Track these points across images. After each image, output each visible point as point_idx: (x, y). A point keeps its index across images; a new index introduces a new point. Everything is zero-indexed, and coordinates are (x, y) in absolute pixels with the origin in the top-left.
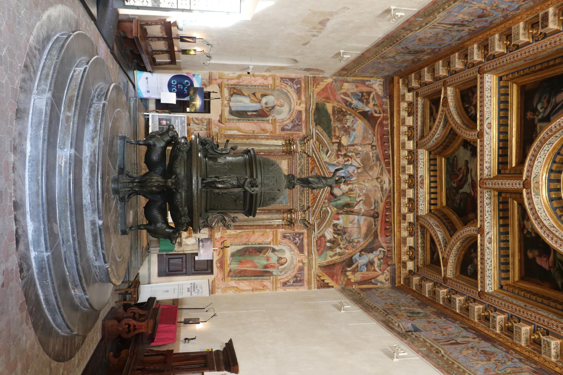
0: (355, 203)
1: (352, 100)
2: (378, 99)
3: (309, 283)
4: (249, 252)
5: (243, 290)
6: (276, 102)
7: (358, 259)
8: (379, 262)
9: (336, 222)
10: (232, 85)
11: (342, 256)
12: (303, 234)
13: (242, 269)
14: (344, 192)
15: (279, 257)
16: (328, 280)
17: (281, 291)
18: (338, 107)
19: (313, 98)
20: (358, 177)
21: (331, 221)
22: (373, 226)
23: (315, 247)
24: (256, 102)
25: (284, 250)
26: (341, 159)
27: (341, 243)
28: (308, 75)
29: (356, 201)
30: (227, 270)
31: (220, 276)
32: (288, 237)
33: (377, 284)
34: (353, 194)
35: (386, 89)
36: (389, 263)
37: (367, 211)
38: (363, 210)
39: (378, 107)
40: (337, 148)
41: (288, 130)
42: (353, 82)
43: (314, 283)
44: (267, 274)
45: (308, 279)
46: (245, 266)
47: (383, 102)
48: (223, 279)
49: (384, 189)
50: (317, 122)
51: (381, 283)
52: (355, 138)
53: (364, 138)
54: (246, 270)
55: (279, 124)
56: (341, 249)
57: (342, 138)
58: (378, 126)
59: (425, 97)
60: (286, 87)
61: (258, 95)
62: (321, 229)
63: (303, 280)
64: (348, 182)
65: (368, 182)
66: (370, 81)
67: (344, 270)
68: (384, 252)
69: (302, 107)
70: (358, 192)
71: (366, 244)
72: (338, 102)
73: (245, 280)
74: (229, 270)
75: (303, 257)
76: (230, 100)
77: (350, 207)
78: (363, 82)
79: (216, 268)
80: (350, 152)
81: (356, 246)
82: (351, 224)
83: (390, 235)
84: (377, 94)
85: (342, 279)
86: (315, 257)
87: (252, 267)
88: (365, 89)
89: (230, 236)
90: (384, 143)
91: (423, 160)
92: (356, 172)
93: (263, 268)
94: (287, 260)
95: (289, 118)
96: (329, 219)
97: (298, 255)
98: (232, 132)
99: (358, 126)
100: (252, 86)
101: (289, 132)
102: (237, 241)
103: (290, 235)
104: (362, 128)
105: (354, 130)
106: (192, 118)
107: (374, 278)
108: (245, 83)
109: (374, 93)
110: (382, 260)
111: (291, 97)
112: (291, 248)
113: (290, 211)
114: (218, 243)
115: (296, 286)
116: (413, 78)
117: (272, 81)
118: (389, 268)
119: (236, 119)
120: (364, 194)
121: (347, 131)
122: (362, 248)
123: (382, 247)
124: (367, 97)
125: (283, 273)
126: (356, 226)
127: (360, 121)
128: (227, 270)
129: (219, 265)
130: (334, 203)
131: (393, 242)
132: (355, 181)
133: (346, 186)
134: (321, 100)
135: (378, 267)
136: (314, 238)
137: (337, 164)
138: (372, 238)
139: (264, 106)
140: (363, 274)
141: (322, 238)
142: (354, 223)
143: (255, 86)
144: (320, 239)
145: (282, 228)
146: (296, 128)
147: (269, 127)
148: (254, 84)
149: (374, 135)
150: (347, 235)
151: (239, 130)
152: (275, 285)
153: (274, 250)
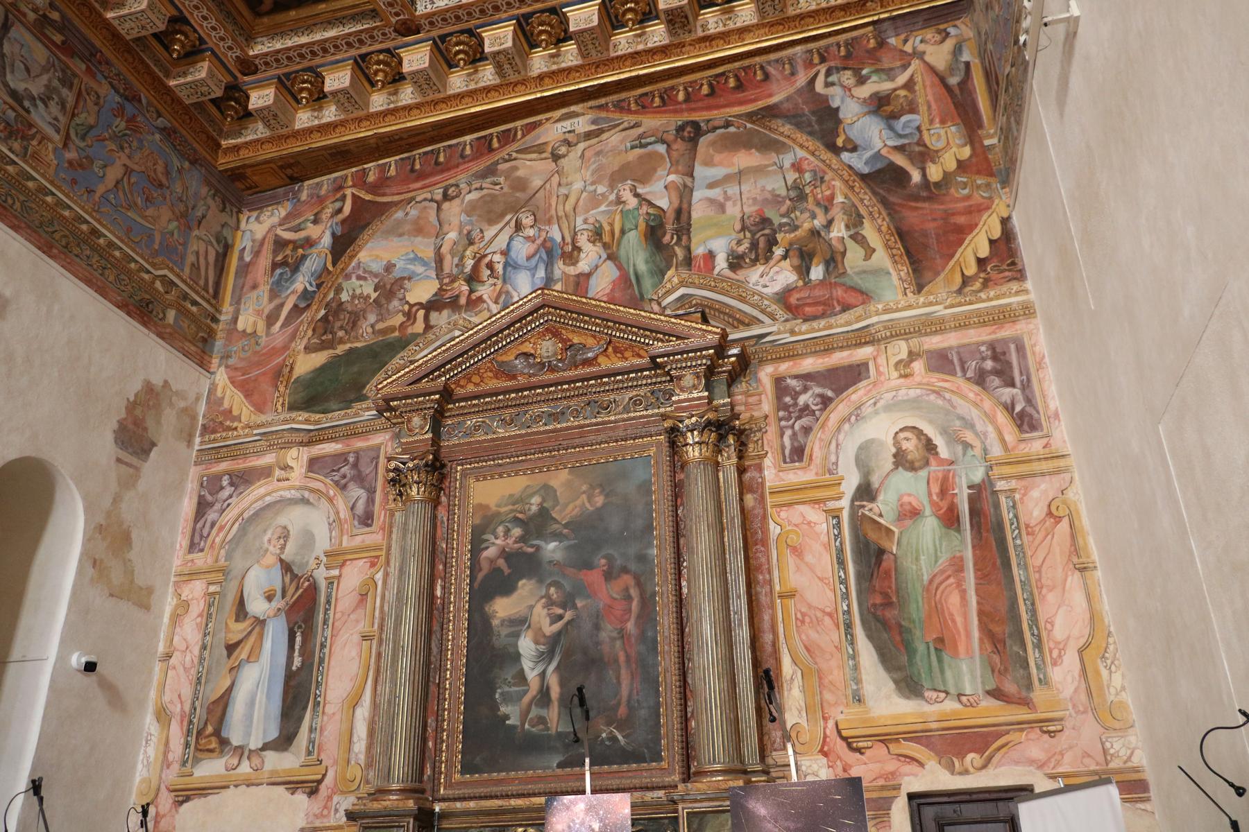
0: (645, 209)
1: (293, 292)
2: (299, 215)
3: (1004, 316)
4: (888, 604)
5: (1094, 617)
6: (270, 559)
7: (868, 154)
8: (874, 78)
9: (721, 263)
10: (187, 745)
11: (863, 211)
12: (778, 381)
13: (976, 634)
14: (604, 256)
15: (897, 464)
16: (979, 244)
17: (1062, 435)
18: (310, 333)
19: (270, 424)
20: (549, 222)
21: (724, 279)
22: (732, 129)
23: (832, 320)
24: (261, 636)
25: (861, 448)
26: (485, 291)
27: (807, 226)
28: (195, 453)
30: (992, 712)
31: (1034, 746)
32: (801, 438)
33: (967, 64)
34: (611, 225)
35: (274, 197)
36: (872, 43)
38: (672, 177)
39: (323, 209)
40: (445, 312)
41: (371, 501)
42: (237, 301)
43: (997, 297)
44: (988, 508)
45: (984, 324)
46: (959, 620)
47: (311, 196)
48: (1048, 727)
49: (594, 127)
50: (352, 396)
51: (957, 50)
52: (417, 259)
53: (419, 230)
54: (981, 613)
55: (345, 538)
56: (830, 223)
57: (412, 302)
58: (384, 195)
59: (250, 39)
60: (221, 528)
61: (238, 630)
62: (755, 313)
63: (992, 346)
66: (245, 248)
67: (924, 194)
68: (829, 73)
69: (297, 458)
70: (603, 208)
71: (801, 137)
72: (293, 337)
73: (1033, 613)
75: (882, 360)
76: (240, 750)
77: (662, 225)
78: (244, 269)
79: (990, 770)
80: (460, 265)
81: (814, 172)
82: (729, 204)
83: (762, 68)
85: (966, 192)
86: (877, 313)
87: (959, 585)
88: (265, 261)
89: (815, 708)
90: (437, 163)
92: (531, 232)
93: (958, 530)
94: (901, 430)
95: (330, 500)
97: (875, 384)
98: (361, 730)
100: (201, 659)
101: (378, 497)
102: (836, 672)
103: (788, 432)
104: (384, 242)
105: (389, 267)
107: (943, 80)
108: (187, 692)
109: (279, 232)
110: (864, 72)
112: (846, 419)
113: (674, 437)
115: (1025, 371)
116: (182, 80)
117: (198, 583)
118: (892, 41)
119: (312, 719)
120: (612, 187)
121: (390, 287)
122: (822, 147)
123: (812, 81)
124: (288, 252)
125: (969, 437)
126: (733, 190)
127: (363, 256)
128: (992, 712)
130: (647, 283)
132: (565, 225)
133: (582, 255)
134: (282, 394)
135: (892, 79)
136: (792, 333)
137: (503, 296)
138: (777, 123)
139: (278, 603)
140: (931, 122)
141: (793, 300)
142: (721, 199)
143: (204, 647)
144: (797, 307)
145: (760, 468)
146: (366, 469)
147: (353, 576)
148: (196, 651)
149: (413, 199)
150: (770, 213)
152: (1036, 467)
153: (866, 492)
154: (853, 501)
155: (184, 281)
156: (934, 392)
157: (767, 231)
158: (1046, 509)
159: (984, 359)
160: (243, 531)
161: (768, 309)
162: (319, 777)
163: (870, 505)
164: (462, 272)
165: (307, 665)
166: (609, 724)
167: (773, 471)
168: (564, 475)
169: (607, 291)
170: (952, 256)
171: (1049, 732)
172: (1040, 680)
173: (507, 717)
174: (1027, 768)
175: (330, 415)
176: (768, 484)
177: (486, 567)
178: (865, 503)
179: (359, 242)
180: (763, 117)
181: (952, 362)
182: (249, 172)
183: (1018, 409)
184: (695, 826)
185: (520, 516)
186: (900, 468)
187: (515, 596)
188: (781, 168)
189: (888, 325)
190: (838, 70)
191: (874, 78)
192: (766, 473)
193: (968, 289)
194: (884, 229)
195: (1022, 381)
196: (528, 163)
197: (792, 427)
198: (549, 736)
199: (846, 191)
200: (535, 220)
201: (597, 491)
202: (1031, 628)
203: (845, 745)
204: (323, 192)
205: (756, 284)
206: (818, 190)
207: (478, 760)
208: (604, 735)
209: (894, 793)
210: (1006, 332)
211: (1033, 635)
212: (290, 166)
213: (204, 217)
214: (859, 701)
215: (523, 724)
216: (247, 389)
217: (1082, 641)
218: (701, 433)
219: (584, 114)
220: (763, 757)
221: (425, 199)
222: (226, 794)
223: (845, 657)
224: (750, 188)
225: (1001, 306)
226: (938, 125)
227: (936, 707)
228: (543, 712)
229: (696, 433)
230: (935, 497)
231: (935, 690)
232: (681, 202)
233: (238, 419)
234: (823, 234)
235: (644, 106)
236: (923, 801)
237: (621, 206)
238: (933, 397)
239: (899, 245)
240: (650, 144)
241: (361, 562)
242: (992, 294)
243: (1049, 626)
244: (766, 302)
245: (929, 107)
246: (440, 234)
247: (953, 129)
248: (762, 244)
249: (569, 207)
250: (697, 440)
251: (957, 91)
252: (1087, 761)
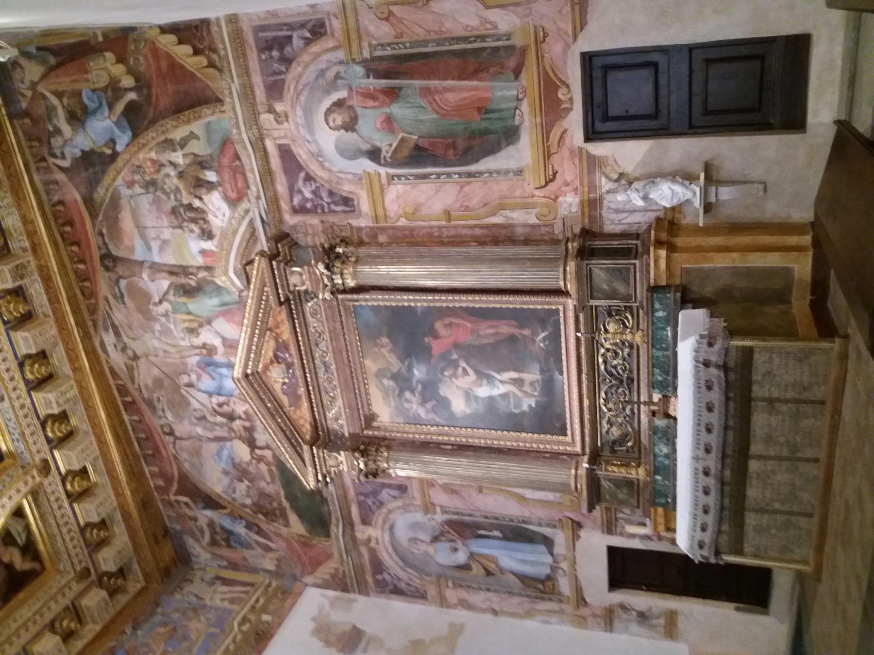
0: (171, 297)
4: (454, 146)
6: (430, 549)
7: (116, 130)
9: (208, 245)
10: (550, 600)
11: (162, 138)
12: (295, 211)
13: (475, 83)
14: (208, 327)
15: (353, 130)
18: (275, 524)
20: (185, 364)
21: (220, 245)
22: (104, 231)
23: (247, 168)
24: (480, 555)
27: (175, 181)
29: (171, 303)
30: (530, 77)
31: (554, 49)
32: (337, 198)
34: (184, 321)
36: (27, 121)
37: (133, 275)
38: (145, 276)
40: (256, 435)
43: (223, 42)
44: (383, 66)
45: (244, 55)
46: (465, 95)
48: (541, 38)
49: (111, 330)
52: (219, 454)
53: (197, 453)
54: (460, 78)
55: (415, 502)
56: (171, 163)
58: (173, 476)
60: (411, 580)
61: (477, 569)
63: (261, 50)
64: (204, 351)
65: (155, 349)
67: (145, 91)
68: (54, 156)
70: (172, 327)
71: (107, 180)
72: (279, 535)
74: (523, 76)
75: (276, 134)
76: (554, 568)
79: (570, 81)
80: (221, 425)
81: (134, 172)
83: (54, 205)
84: (198, 541)
86: (240, 134)
88: (226, 552)
90: (147, 439)
92: (194, 377)
93: (400, 89)
94: (328, 124)
95: (390, 512)
96: (229, 253)
97: (294, 141)
100: (496, 591)
103: (333, 207)
105: (226, 473)
108: (516, 600)
110: (51, 129)
111: (395, 557)
112: (322, 165)
114: (569, 179)
115: (280, 27)
120: (155, 319)
121: (241, 472)
124: (218, 538)
125: (331, 74)
126: (152, 233)
128: (530, 77)
129: (561, 94)
130: (227, 298)
131: (39, 184)
133: (209, 342)
134: (320, 543)
139: (459, 544)
140: (87, 80)
142: (159, 242)
143: (488, 590)
144: (238, 192)
145: (359, 229)
148: (491, 594)
149: (174, 456)
151: (522, 499)
153: (374, 154)
154: (380, 164)
155: (242, 608)
156: (298, 97)
157: (182, 210)
158: (384, 22)
159: (271, 57)
160: (413, 566)
161: (242, 213)
162: (570, 521)
163: (384, 153)
164: (226, 425)
165: (499, 528)
166: (534, 341)
167: (361, 220)
168: (368, 363)
169: (235, 326)
170: (193, 74)
171: (544, 37)
172: (507, 39)
173: (530, 406)
174: (569, 55)
175: (332, 511)
176: (371, 224)
177: (431, 416)
178: (382, 156)
179: (209, 492)
180: (93, 207)
181: (275, 82)
182: (162, 565)
183: (308, 35)
184: (600, 296)
185: (397, 392)
186: (356, 127)
187: (450, 397)
188: (131, 197)
189: (249, 128)
190: (50, 148)
191: (55, 121)
192: (363, 225)
193: (218, 64)
194: (174, 123)
195: (288, 30)
196: (141, 377)
197: (329, 204)
198: (543, 380)
199: (146, 149)
200: (185, 373)
201: (378, 341)
202: (470, 42)
203: (550, 184)
204: (174, 515)
205: (223, 221)
206: (147, 170)
207: (558, 425)
208: (542, 345)
209: (584, 152)
210: (250, 38)
211: (475, 41)
212: (156, 538)
213: (196, 596)
214: (521, 171)
215: (535, 396)
216: (316, 564)
217: (481, 6)
218: (333, 273)
219: (101, 337)
220: (556, 242)
221: (174, 448)
222: (580, 576)
223: (491, 179)
224: (150, 220)
225: (230, 41)
226: (90, 76)
227: (526, 117)
228: (527, 383)
229: (334, 277)
230: (377, 104)
231: (514, 116)
232: (163, 271)
233: (337, 570)
234: (180, 169)
235: (90, 294)
236: (591, 130)
237: (170, 314)
238: (302, 98)
239: (186, 113)
240: (120, 290)
241: (431, 492)
242: (221, 46)
243: (468, 29)
244: (236, 215)
245: (75, 81)
246: (200, 438)
247: (91, 64)
248: (192, 215)
249: (173, 350)
250: (339, 276)
251: (61, 59)
252: (564, 12)
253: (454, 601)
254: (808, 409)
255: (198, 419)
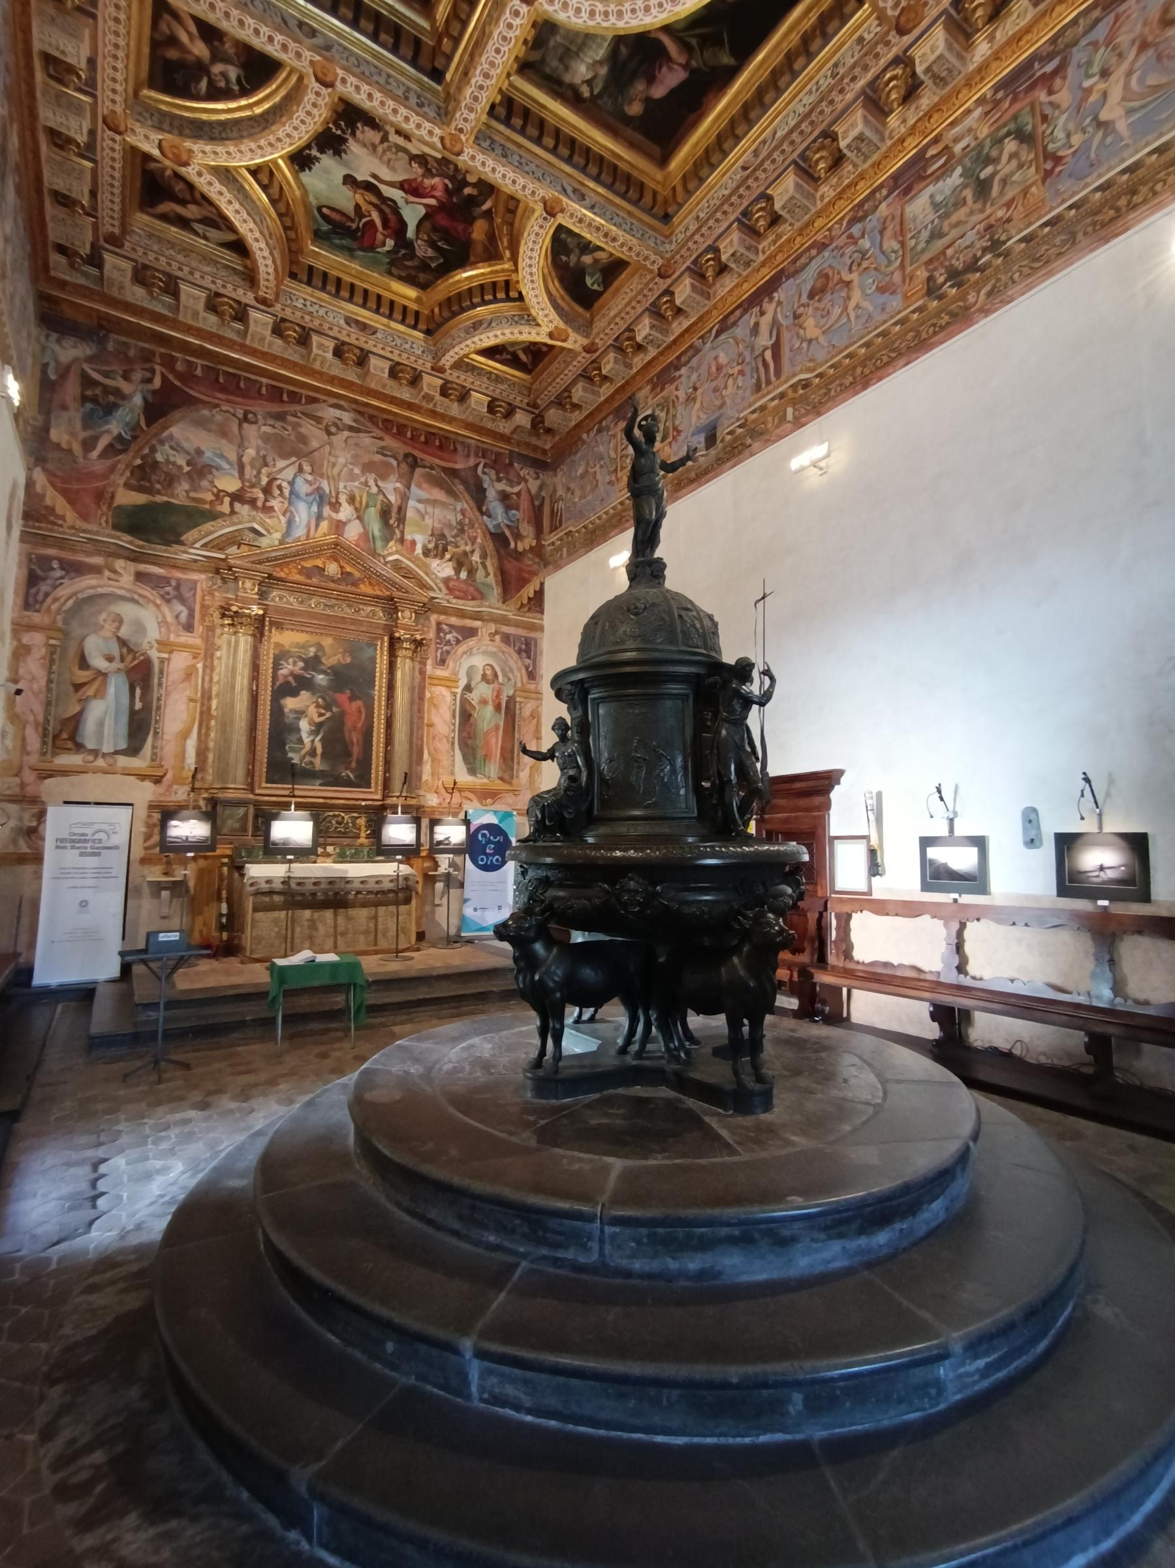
41: (191, 615)
91: (308, 303)
99: (187, 439)
106: (146, 849)
119: (154, 742)
121: (200, 470)
127: (177, 431)
136: (448, 602)
151: (184, 735)
165: (147, 707)
253: (26, 639)
254: (371, 937)
255: (264, 457)
